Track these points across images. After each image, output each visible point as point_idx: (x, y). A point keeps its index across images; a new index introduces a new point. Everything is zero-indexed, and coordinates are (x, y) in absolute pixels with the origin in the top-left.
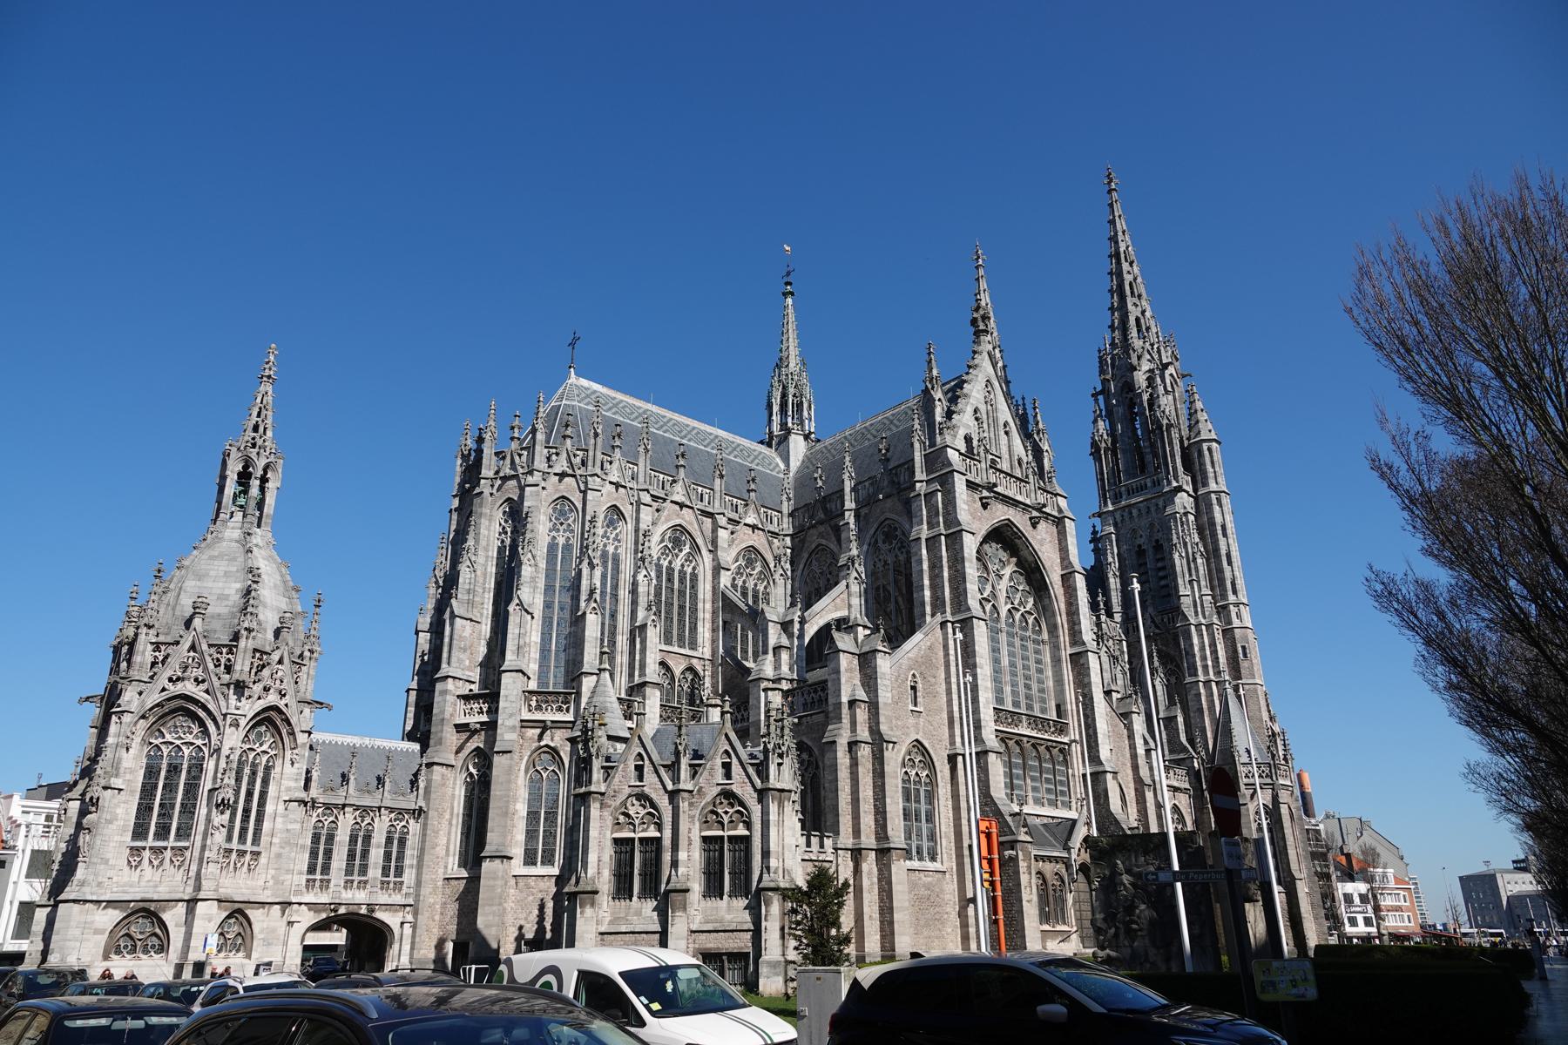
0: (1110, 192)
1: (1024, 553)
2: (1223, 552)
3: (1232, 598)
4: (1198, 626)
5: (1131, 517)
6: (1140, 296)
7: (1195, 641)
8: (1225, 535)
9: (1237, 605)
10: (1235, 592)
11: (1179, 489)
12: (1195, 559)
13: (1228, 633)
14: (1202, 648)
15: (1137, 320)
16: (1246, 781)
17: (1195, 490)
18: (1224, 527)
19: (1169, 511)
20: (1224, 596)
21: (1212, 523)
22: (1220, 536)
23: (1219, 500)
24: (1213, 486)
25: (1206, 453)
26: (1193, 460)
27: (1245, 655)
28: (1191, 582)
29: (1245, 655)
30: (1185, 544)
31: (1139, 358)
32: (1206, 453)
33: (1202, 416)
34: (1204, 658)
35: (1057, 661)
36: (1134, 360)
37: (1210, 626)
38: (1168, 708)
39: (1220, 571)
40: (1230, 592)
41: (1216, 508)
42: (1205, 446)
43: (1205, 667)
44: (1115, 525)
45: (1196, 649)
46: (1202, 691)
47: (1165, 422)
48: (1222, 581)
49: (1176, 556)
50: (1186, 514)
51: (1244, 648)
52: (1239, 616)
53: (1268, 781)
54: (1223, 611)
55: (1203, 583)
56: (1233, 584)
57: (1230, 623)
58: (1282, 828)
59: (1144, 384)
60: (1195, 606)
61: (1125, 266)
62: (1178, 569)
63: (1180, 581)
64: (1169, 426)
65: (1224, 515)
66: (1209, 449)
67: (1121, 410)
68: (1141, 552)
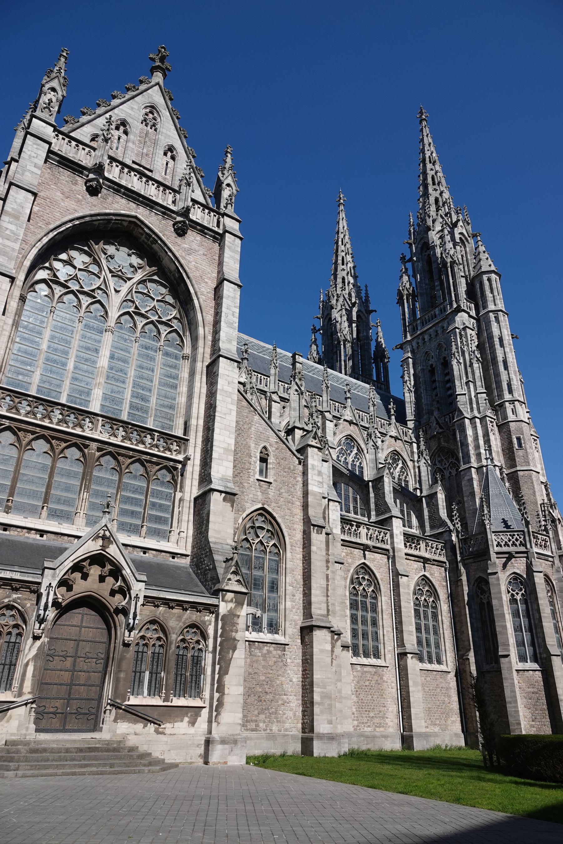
0: (421, 122)
1: (166, 262)
2: (500, 358)
3: (507, 396)
4: (472, 420)
5: (424, 343)
6: (439, 183)
7: (470, 432)
8: (502, 345)
9: (512, 402)
10: (510, 391)
11: (459, 310)
12: (471, 365)
13: (504, 428)
14: (476, 439)
15: (437, 200)
16: (497, 549)
17: (478, 312)
18: (501, 339)
19: (451, 328)
20: (501, 396)
21: (490, 337)
22: (497, 346)
23: (497, 319)
24: (491, 307)
25: (486, 283)
26: (475, 293)
27: (520, 445)
28: (467, 383)
29: (520, 445)
30: (463, 352)
31: (434, 221)
32: (486, 283)
33: (483, 256)
34: (477, 447)
35: (192, 374)
36: (430, 222)
37: (482, 419)
38: (431, 487)
39: (497, 375)
40: (506, 392)
41: (494, 326)
42: (485, 277)
43: (479, 455)
44: (413, 352)
45: (470, 439)
46: (475, 476)
47: (449, 260)
48: (499, 383)
49: (454, 362)
50: (464, 329)
51: (519, 439)
52: (514, 412)
53: (523, 549)
54: (498, 408)
55: (478, 383)
56: (509, 385)
57: (506, 417)
58: (536, 598)
59: (438, 242)
60: (471, 403)
61: (429, 166)
62: (456, 373)
63: (457, 383)
64: (453, 263)
65: (501, 329)
66: (489, 280)
67: (420, 264)
68: (432, 371)
